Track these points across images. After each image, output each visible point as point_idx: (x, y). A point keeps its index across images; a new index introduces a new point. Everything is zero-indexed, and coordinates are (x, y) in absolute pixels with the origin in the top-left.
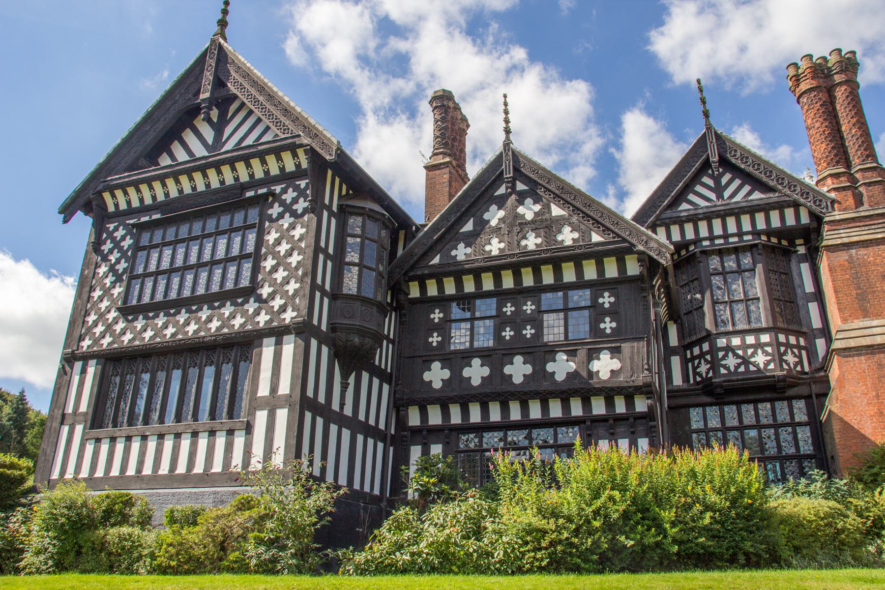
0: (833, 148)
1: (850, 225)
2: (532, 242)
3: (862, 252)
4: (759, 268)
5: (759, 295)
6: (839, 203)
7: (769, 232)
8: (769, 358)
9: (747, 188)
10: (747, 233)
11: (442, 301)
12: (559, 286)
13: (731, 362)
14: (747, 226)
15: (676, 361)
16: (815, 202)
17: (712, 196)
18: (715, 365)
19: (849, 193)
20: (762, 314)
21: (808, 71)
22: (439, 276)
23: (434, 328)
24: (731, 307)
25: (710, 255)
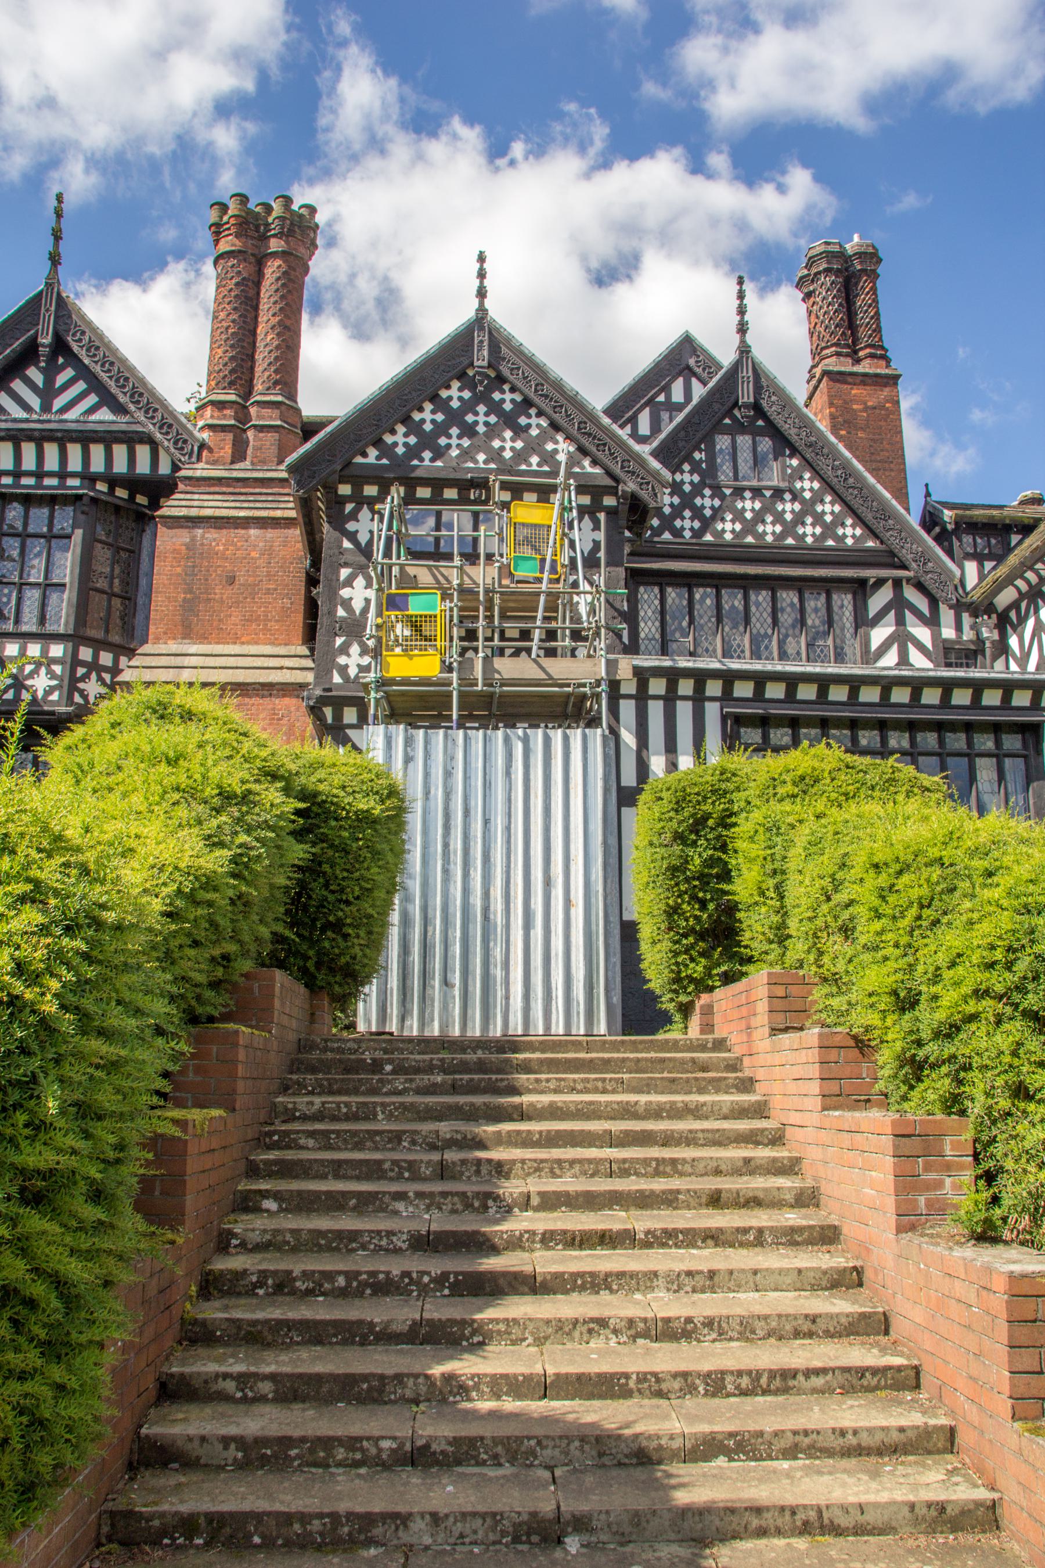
0: (232, 358)
1: (202, 489)
3: (212, 534)
4: (79, 533)
5: (67, 580)
6: (211, 450)
7: (113, 481)
8: (55, 682)
10: (74, 475)
14: (75, 464)
16: (176, 443)
17: (35, 402)
19: (230, 436)
20: (62, 611)
21: (233, 221)
24: (20, 592)
25: (10, 502)
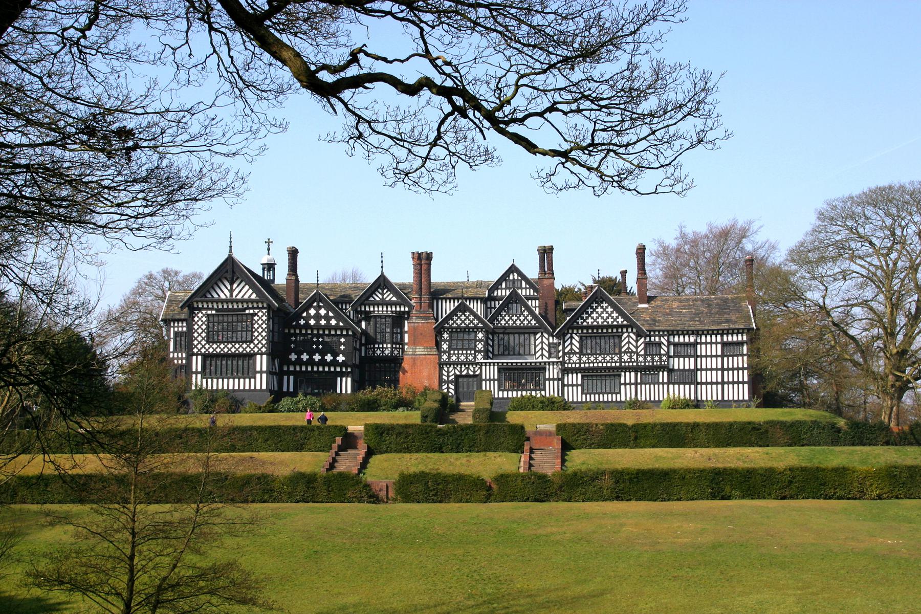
2: (323, 322)
11: (295, 335)
12: (329, 335)
13: (379, 352)
15: (363, 348)
18: (374, 352)
22: (295, 328)
23: (292, 342)
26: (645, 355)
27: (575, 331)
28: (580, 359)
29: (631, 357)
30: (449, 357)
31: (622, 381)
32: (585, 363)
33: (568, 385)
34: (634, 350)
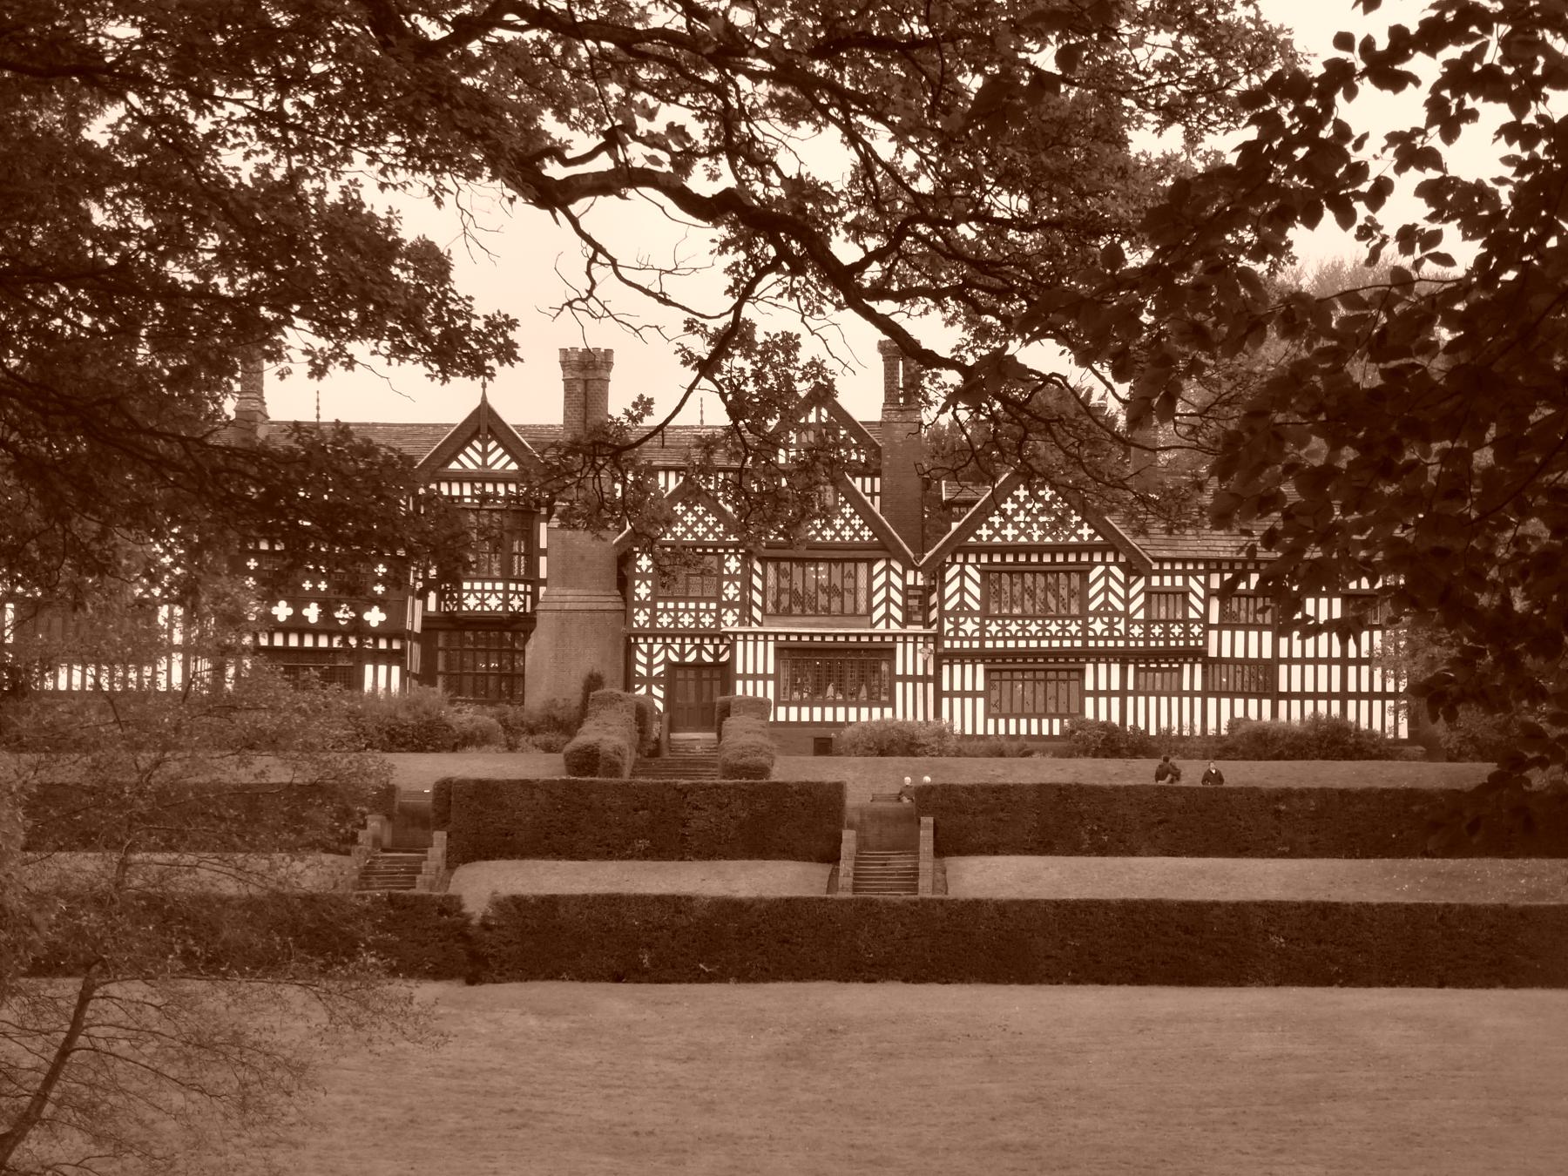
9: (507, 458)
13: (472, 602)
17: (479, 460)
26: (1148, 622)
27: (972, 559)
28: (983, 628)
29: (1111, 626)
30: (653, 618)
31: (1089, 686)
32: (994, 638)
33: (951, 694)
34: (1121, 607)
